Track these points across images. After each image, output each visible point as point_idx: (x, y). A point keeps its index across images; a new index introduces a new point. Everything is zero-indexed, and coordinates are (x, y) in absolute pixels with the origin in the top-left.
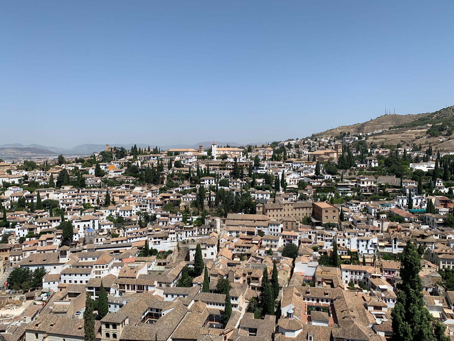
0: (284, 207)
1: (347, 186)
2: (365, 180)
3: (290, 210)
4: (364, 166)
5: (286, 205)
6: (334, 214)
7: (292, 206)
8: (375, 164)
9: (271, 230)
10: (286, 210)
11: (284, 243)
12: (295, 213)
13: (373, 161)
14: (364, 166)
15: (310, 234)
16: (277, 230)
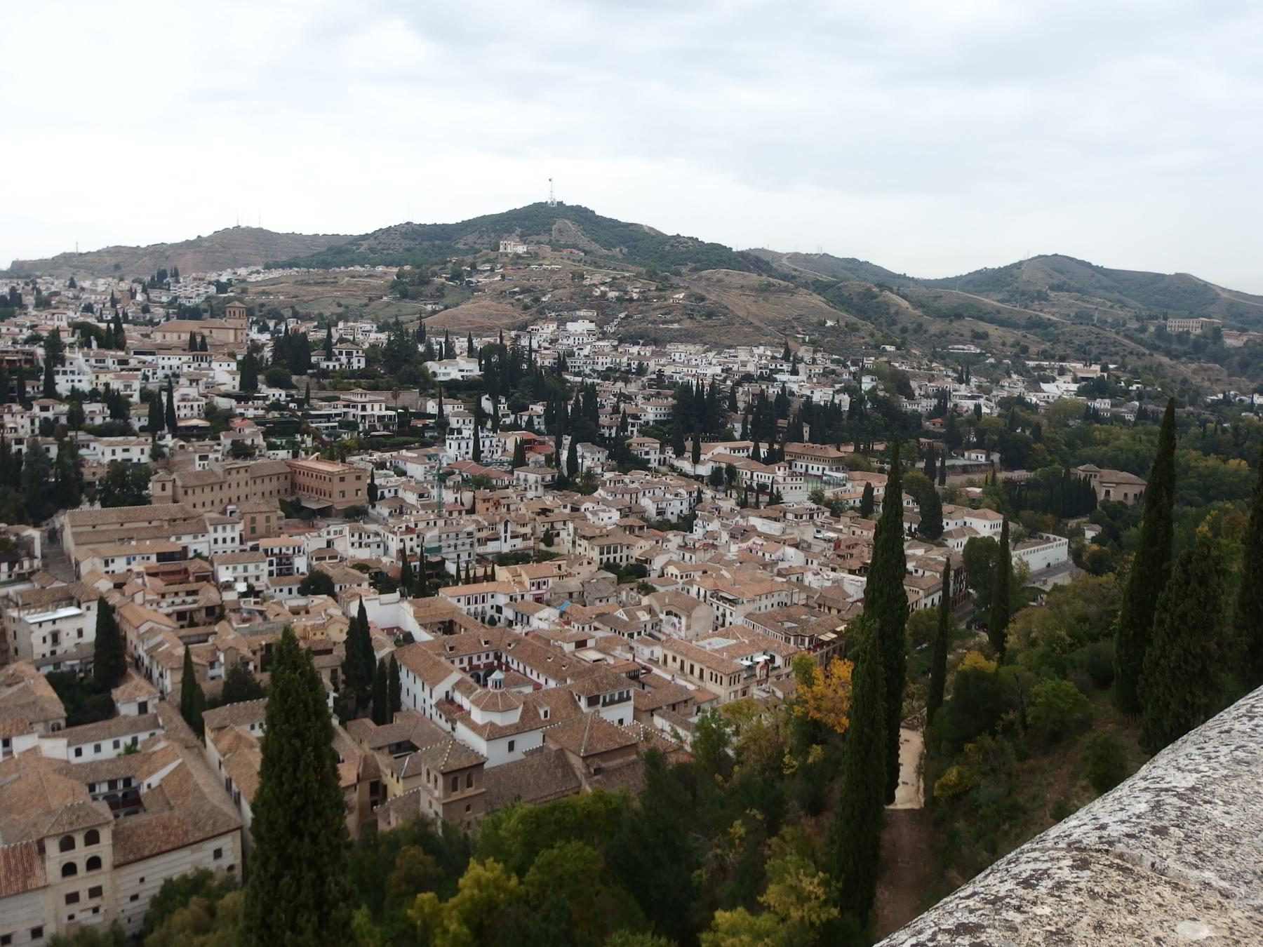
0: (229, 477)
1: (328, 417)
2: (367, 400)
3: (242, 484)
4: (334, 366)
5: (234, 472)
6: (359, 484)
7: (247, 475)
8: (359, 362)
9: (216, 541)
10: (234, 485)
11: (271, 568)
12: (253, 491)
13: (355, 352)
14: (334, 366)
15: (329, 537)
16: (233, 539)
